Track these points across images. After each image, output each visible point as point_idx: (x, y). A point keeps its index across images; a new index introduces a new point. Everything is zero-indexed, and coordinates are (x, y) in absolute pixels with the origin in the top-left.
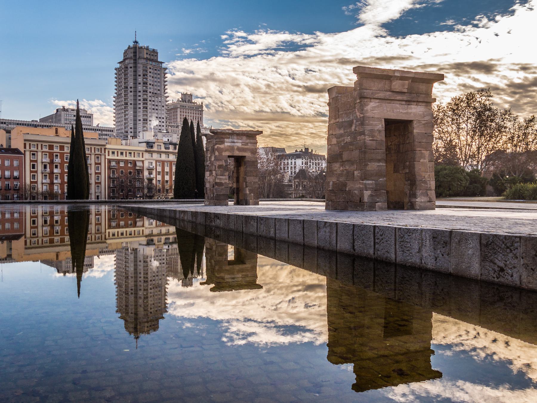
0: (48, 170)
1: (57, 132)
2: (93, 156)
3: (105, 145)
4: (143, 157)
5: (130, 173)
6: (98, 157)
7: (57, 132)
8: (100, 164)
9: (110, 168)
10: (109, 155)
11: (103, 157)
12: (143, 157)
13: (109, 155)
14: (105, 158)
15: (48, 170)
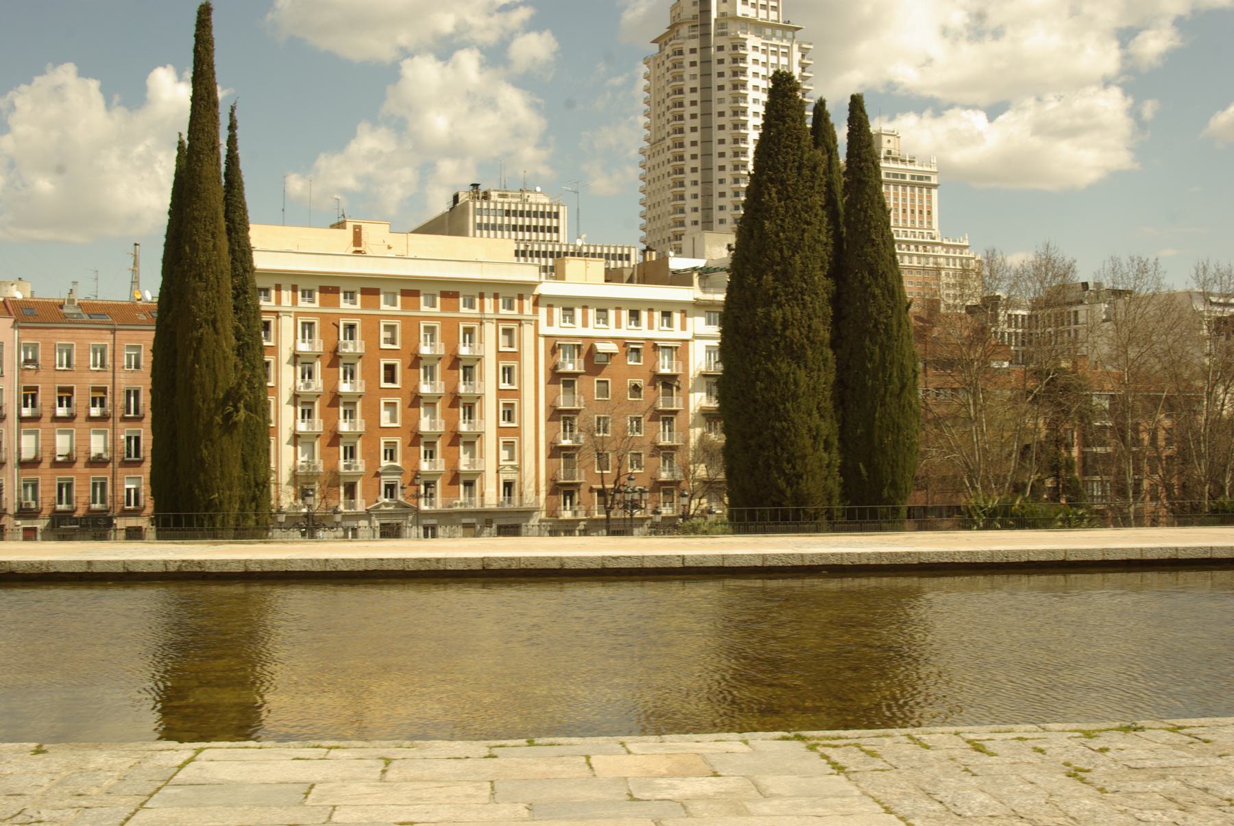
0: (317, 384)
1: (357, 239)
2: (490, 329)
3: (532, 286)
4: (683, 328)
5: (636, 389)
6: (508, 332)
7: (357, 239)
8: (516, 356)
9: (556, 376)
10: (550, 323)
11: (528, 330)
12: (683, 328)
13: (550, 323)
14: (537, 335)
15: (317, 384)
